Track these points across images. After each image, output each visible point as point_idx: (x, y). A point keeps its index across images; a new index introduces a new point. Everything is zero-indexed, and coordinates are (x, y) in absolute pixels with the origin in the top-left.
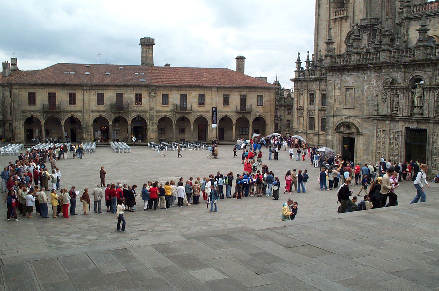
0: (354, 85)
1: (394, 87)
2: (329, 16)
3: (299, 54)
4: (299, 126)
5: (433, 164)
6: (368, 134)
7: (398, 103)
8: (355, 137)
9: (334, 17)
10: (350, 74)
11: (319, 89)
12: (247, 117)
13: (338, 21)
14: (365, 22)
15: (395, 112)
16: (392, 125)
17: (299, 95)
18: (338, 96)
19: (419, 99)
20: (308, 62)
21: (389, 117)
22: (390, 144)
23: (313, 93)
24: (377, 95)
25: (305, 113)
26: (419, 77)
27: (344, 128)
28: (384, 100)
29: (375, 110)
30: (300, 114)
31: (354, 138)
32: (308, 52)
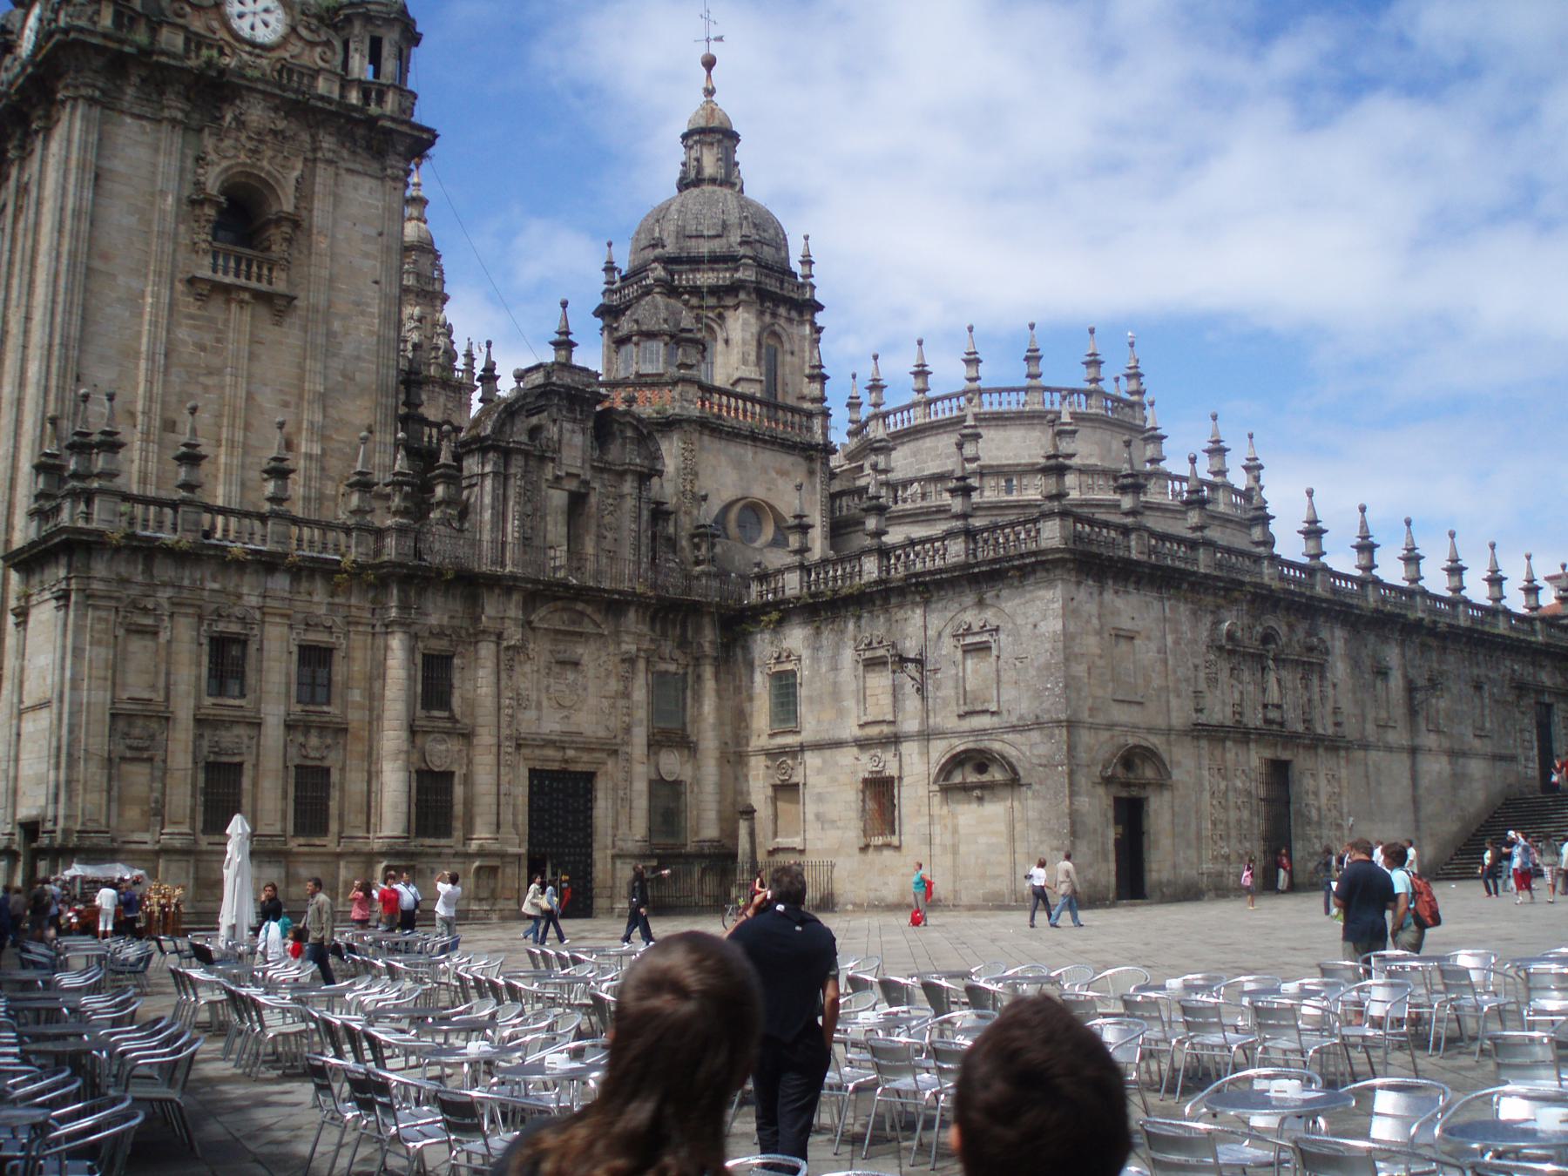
4: (120, 815)
13: (241, 302)
14: (577, 378)
15: (1237, 717)
17: (121, 632)
18: (1096, 659)
23: (234, 628)
24: (1196, 667)
28: (1213, 681)
30: (135, 743)
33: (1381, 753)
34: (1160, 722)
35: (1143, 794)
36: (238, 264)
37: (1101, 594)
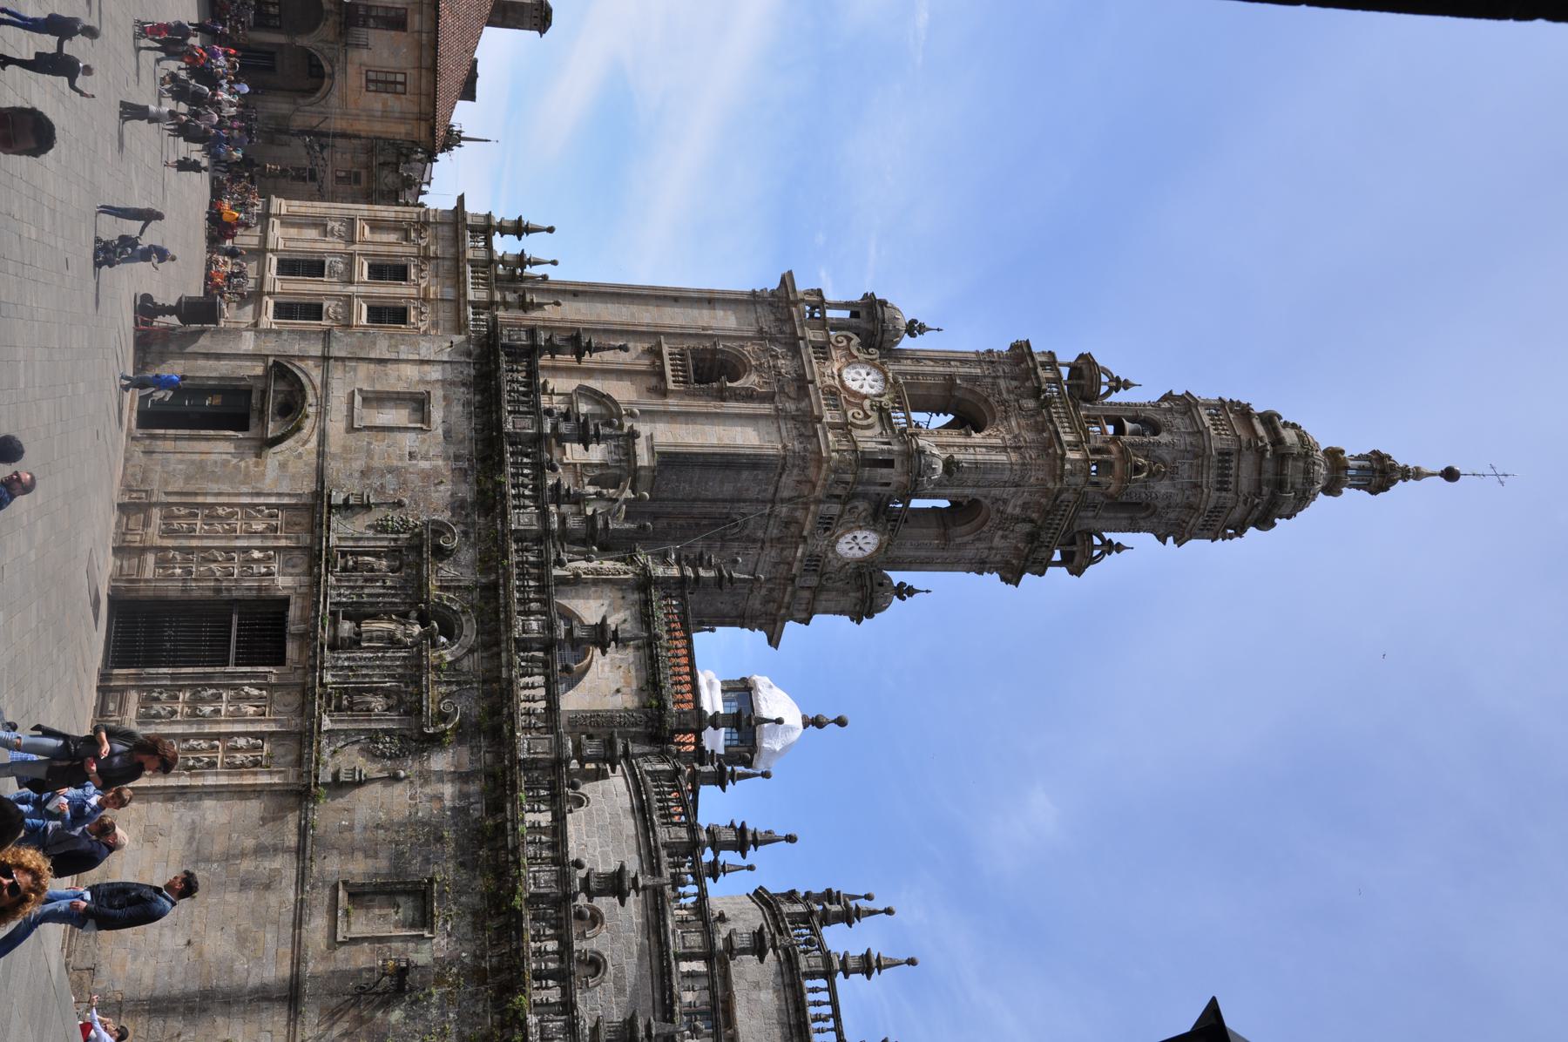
0: (433, 426)
1: (425, 556)
2: (668, 335)
3: (551, 230)
5: (161, 693)
6: (263, 475)
7: (372, 570)
8: (253, 432)
9: (666, 350)
10: (471, 413)
11: (424, 299)
12: (327, 30)
13: (654, 363)
15: (340, 562)
16: (296, 553)
19: (386, 634)
20: (521, 260)
21: (324, 544)
22: (228, 550)
24: (400, 504)
25: (341, 247)
26: (456, 631)
27: (282, 392)
28: (381, 528)
29: (346, 500)
31: (244, 427)
32: (554, 263)
33: (291, 895)
34: (334, 446)
35: (253, 421)
36: (680, 365)
37: (464, 385)
